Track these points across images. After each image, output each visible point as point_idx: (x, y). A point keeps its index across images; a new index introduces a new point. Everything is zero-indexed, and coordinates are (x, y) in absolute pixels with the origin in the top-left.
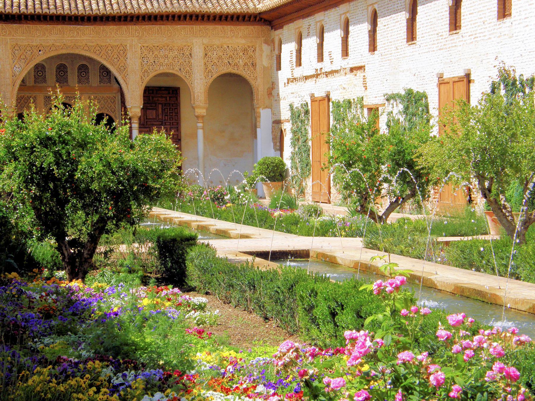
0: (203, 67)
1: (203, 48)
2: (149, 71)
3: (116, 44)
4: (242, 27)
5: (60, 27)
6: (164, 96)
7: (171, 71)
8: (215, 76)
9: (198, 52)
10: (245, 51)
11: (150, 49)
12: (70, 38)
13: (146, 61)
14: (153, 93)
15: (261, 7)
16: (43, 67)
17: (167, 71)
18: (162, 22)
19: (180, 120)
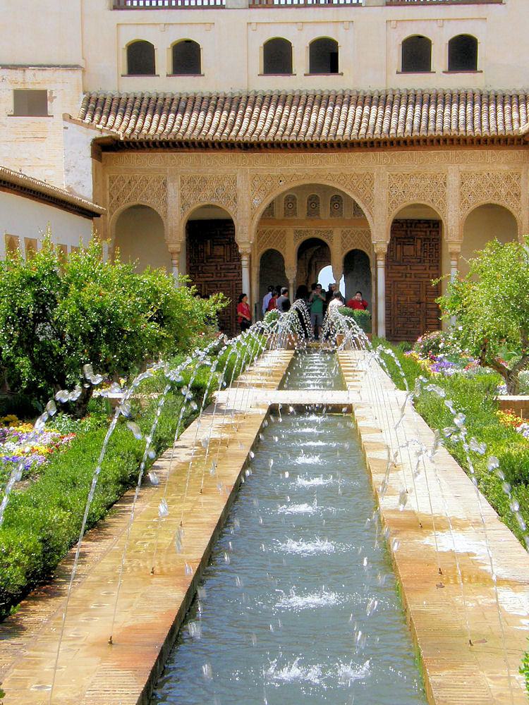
1: (458, 175)
2: (397, 202)
3: (361, 173)
4: (505, 152)
5: (302, 155)
6: (425, 230)
7: (422, 202)
8: (472, 208)
9: (453, 180)
10: (508, 178)
12: (312, 167)
13: (394, 191)
14: (411, 227)
16: (294, 198)
17: (418, 202)
18: (413, 148)
19: (441, 258)
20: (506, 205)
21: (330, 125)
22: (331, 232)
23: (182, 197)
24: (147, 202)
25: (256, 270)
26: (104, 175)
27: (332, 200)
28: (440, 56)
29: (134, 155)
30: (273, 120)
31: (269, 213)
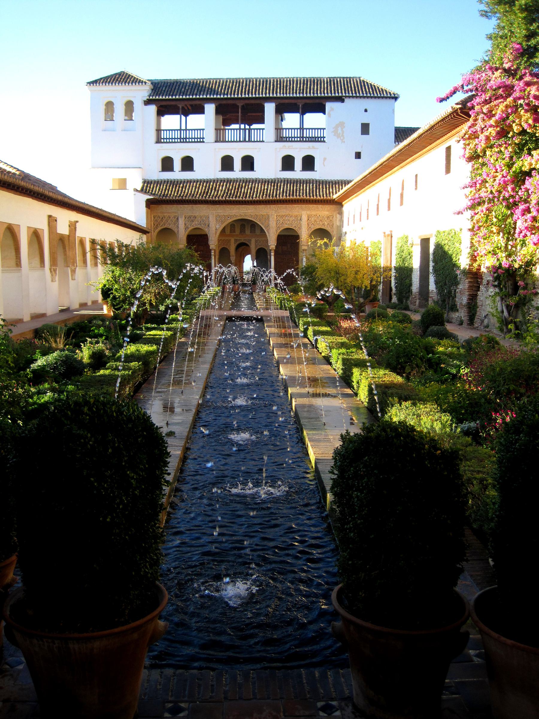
0: (306, 226)
4: (327, 206)
8: (313, 230)
9: (305, 218)
10: (328, 217)
11: (282, 216)
15: (335, 196)
16: (234, 225)
20: (327, 229)
21: (250, 193)
22: (251, 240)
23: (185, 224)
24: (170, 227)
25: (217, 257)
26: (151, 215)
27: (251, 226)
28: (298, 164)
29: (164, 206)
30: (225, 191)
31: (223, 230)
